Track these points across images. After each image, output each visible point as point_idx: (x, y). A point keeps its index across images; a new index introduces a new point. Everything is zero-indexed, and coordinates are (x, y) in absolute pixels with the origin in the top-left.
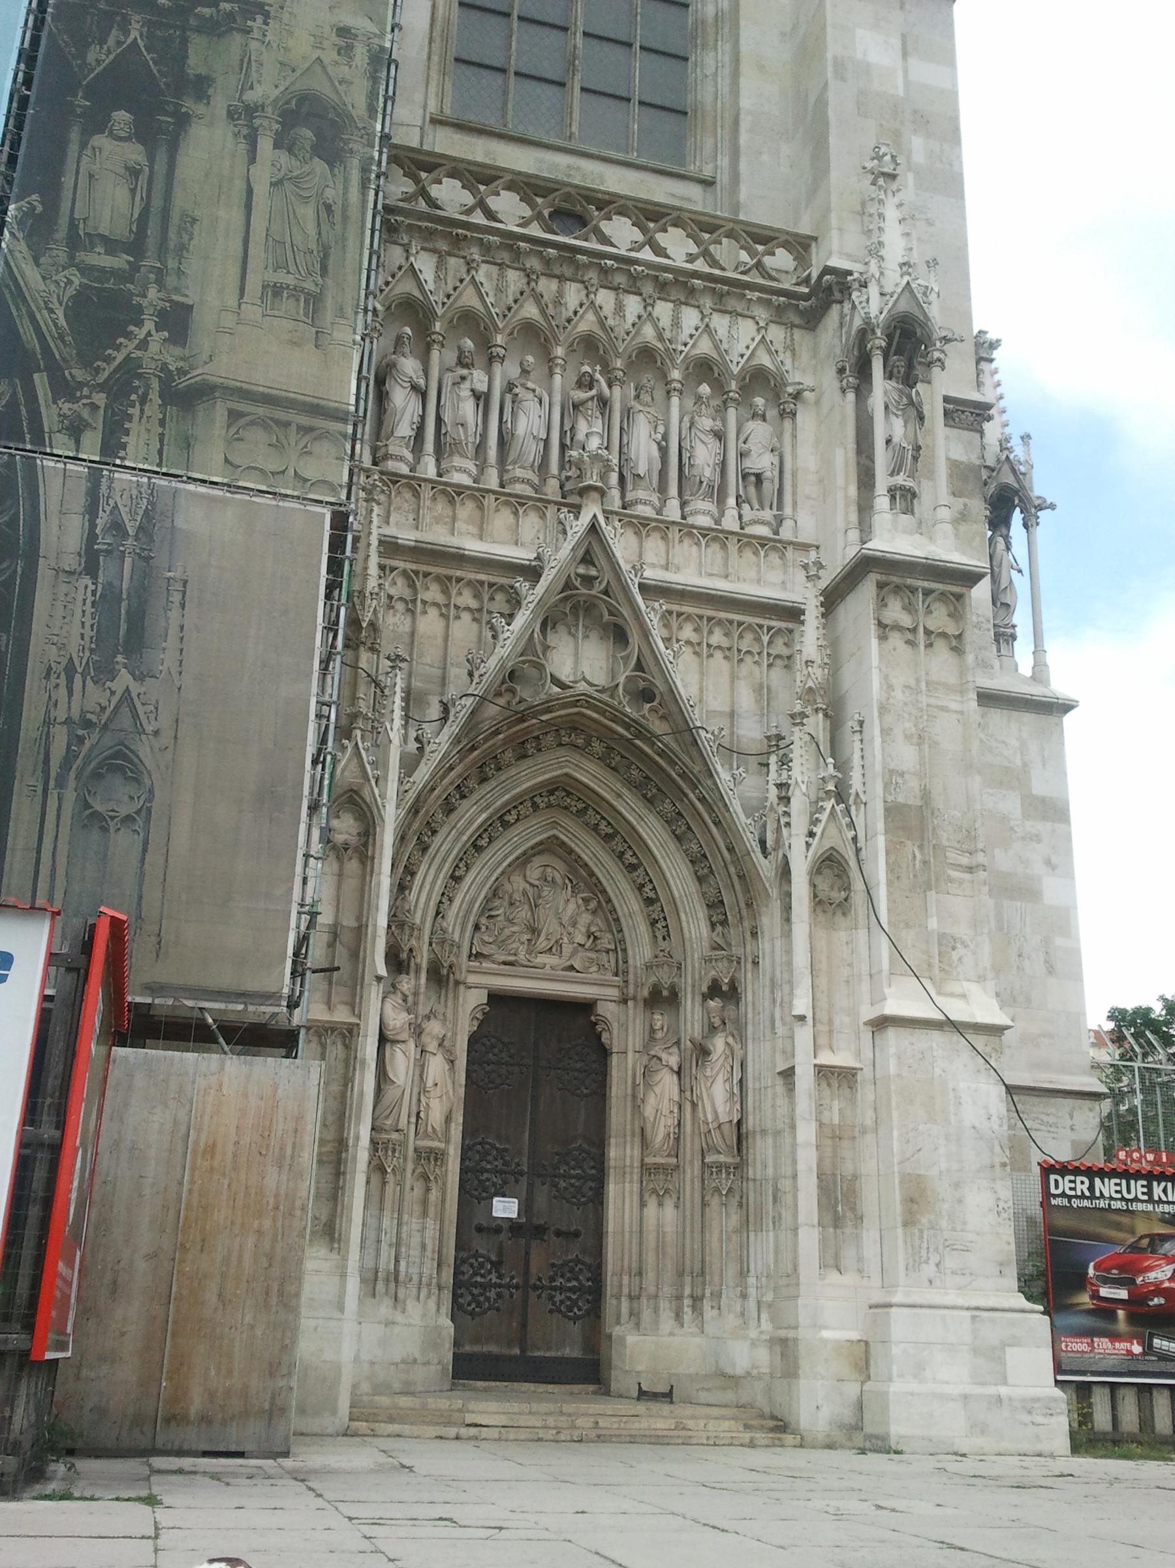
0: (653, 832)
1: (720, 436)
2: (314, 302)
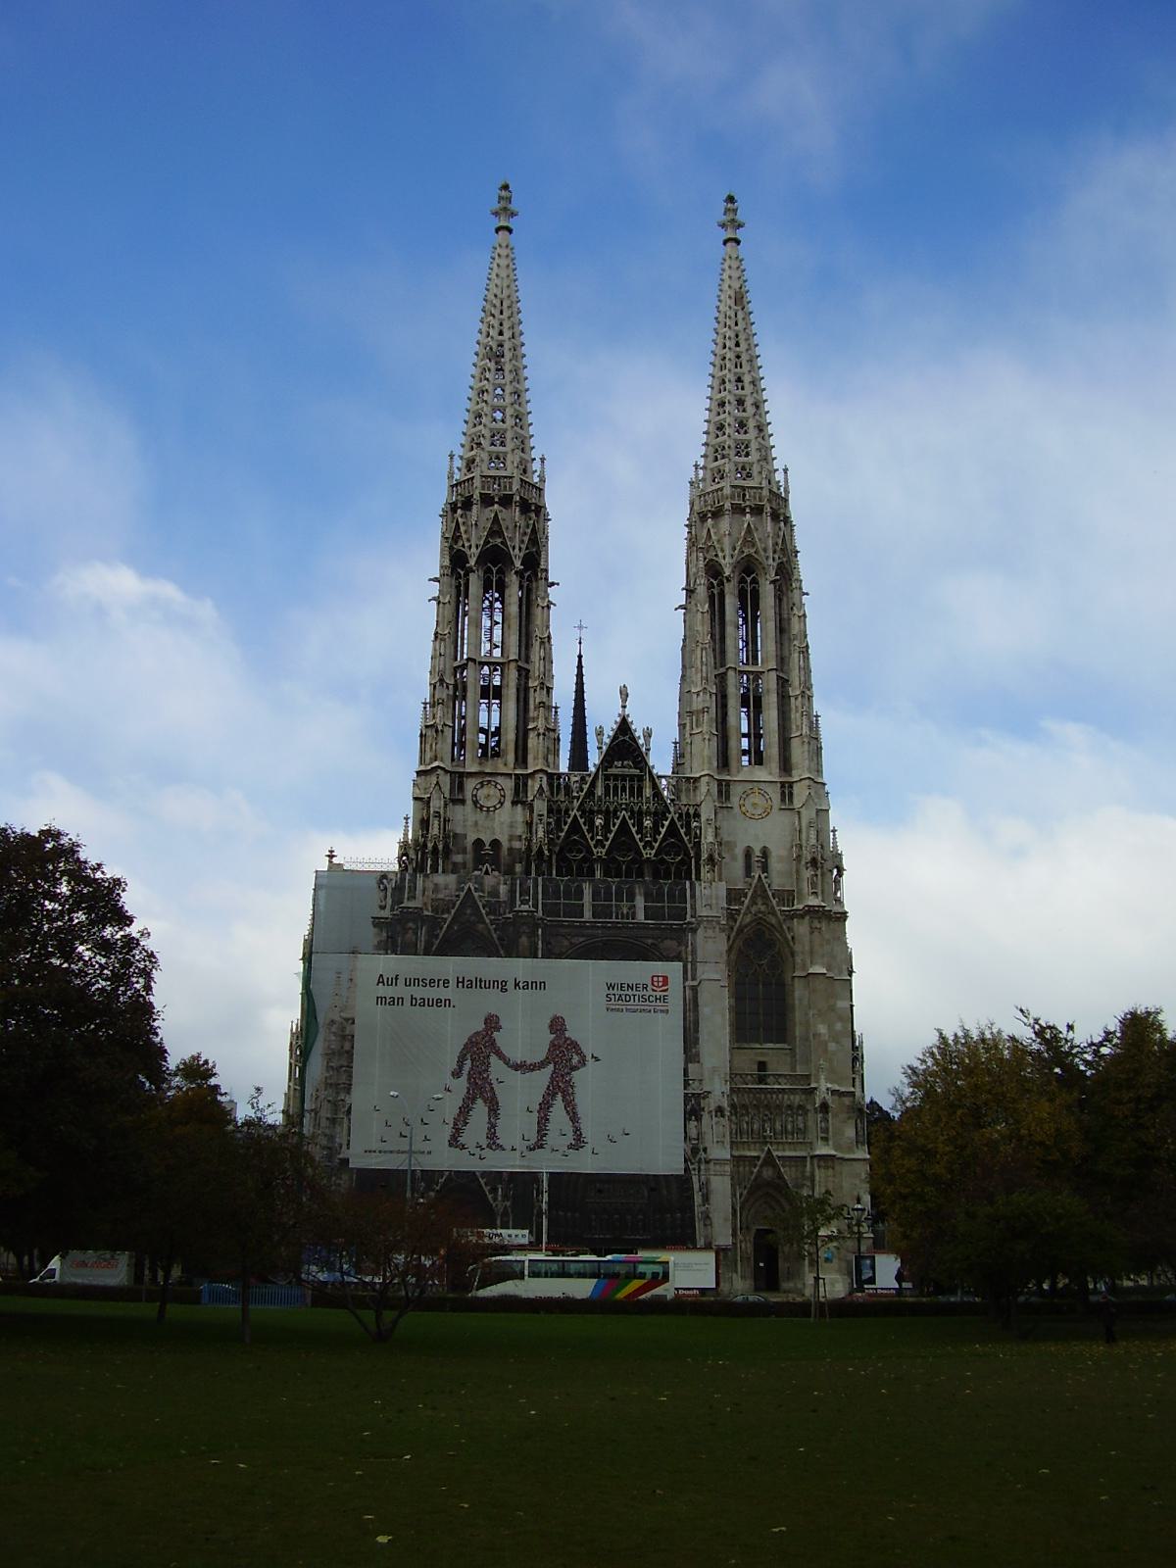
0: (782, 1200)
1: (793, 1122)
2: (723, 1142)
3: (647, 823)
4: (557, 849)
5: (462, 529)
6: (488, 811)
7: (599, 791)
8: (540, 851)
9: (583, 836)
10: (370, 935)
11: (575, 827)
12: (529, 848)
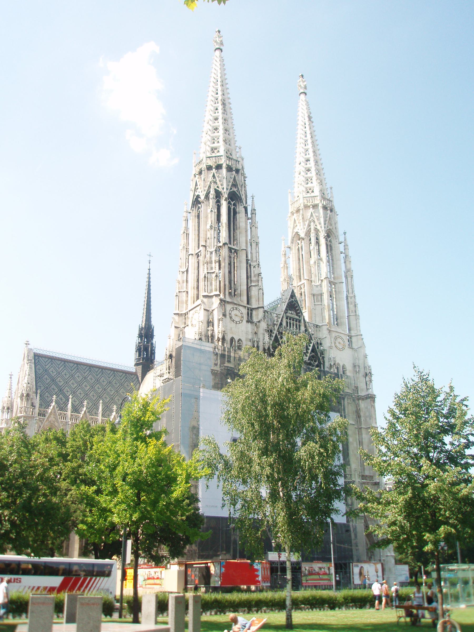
6: (236, 323)
7: (284, 324)
8: (269, 348)
10: (210, 380)
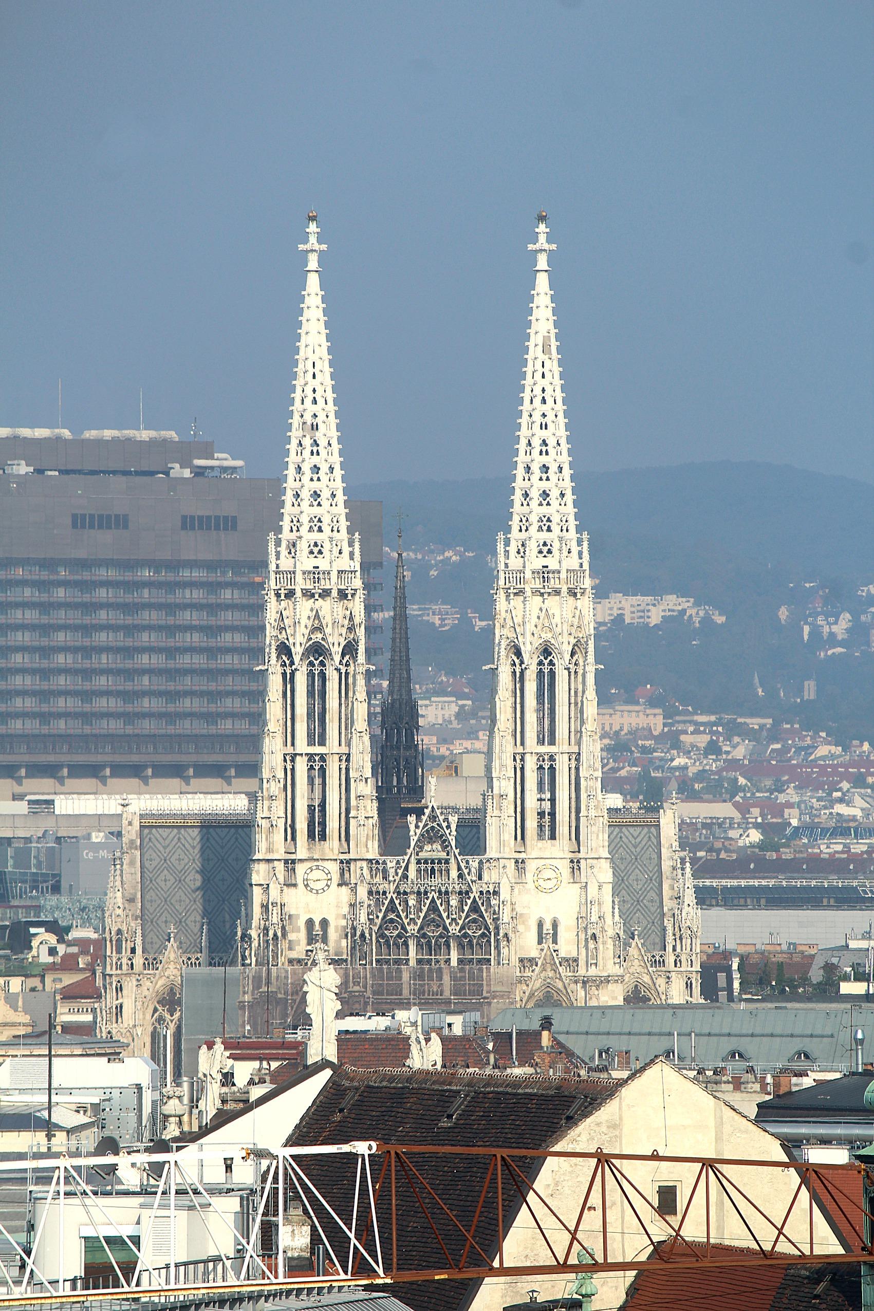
3: (454, 902)
4: (376, 928)
5: (286, 621)
7: (412, 874)
9: (399, 916)
11: (392, 908)
12: (354, 928)
